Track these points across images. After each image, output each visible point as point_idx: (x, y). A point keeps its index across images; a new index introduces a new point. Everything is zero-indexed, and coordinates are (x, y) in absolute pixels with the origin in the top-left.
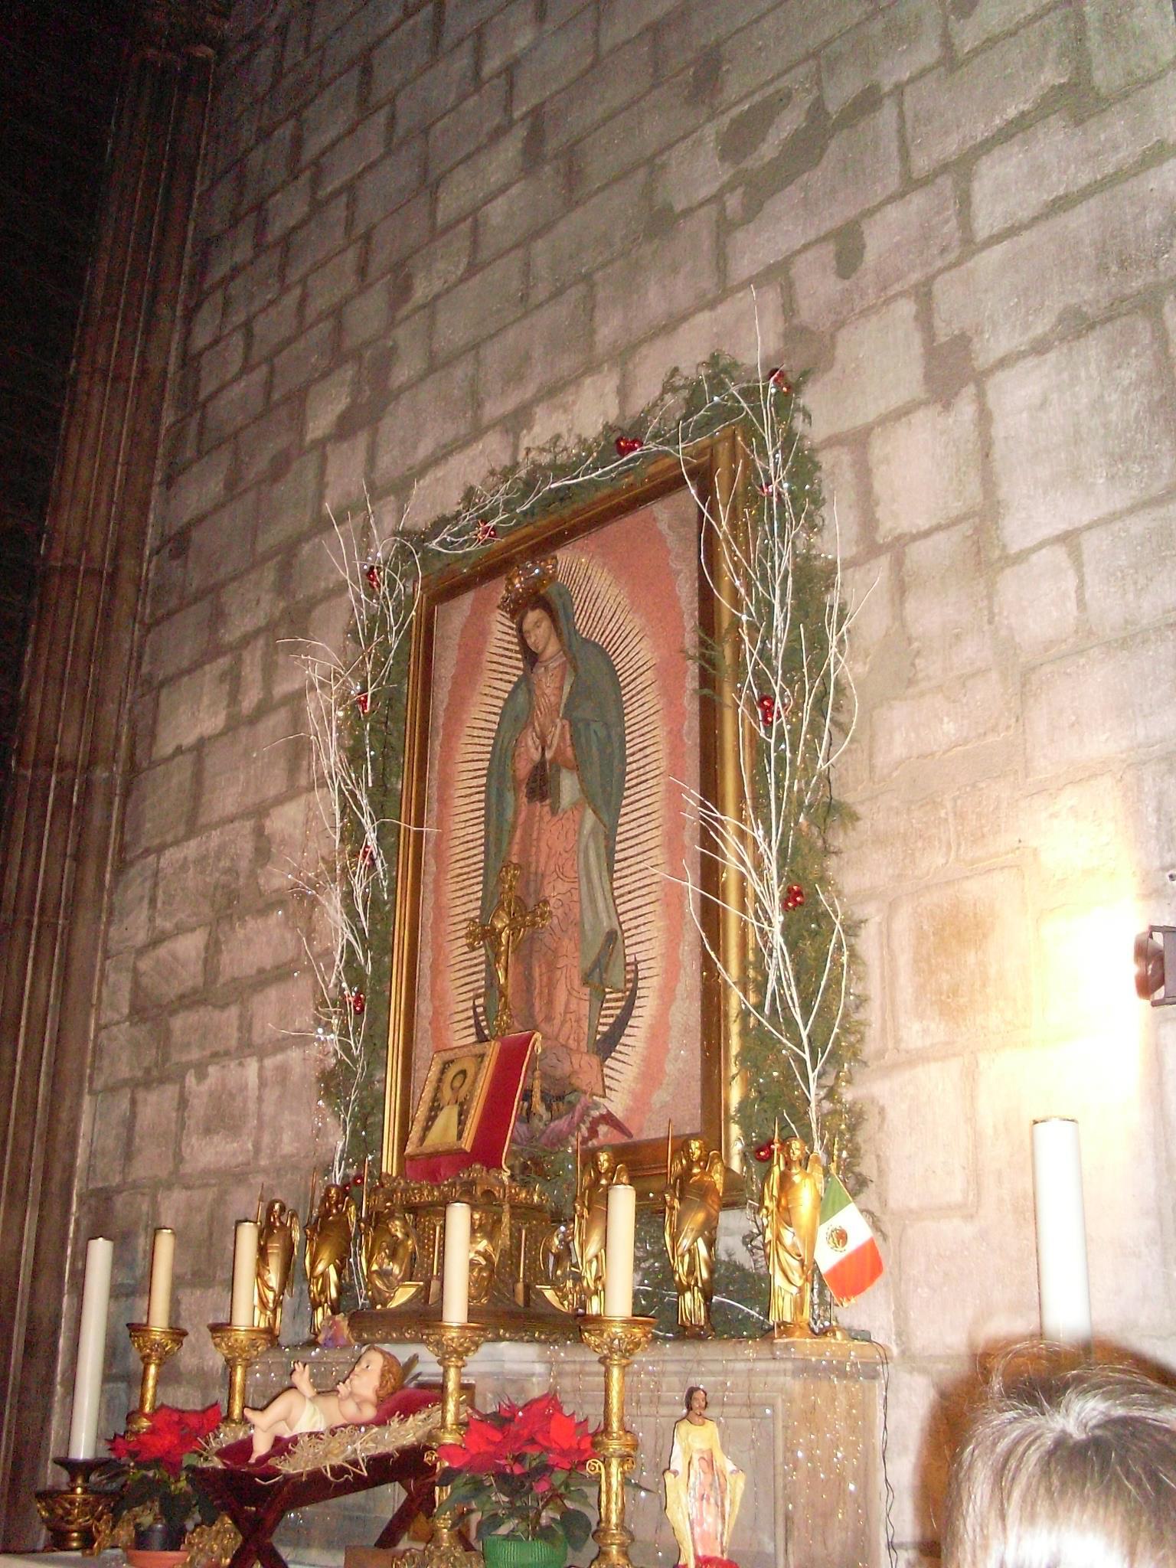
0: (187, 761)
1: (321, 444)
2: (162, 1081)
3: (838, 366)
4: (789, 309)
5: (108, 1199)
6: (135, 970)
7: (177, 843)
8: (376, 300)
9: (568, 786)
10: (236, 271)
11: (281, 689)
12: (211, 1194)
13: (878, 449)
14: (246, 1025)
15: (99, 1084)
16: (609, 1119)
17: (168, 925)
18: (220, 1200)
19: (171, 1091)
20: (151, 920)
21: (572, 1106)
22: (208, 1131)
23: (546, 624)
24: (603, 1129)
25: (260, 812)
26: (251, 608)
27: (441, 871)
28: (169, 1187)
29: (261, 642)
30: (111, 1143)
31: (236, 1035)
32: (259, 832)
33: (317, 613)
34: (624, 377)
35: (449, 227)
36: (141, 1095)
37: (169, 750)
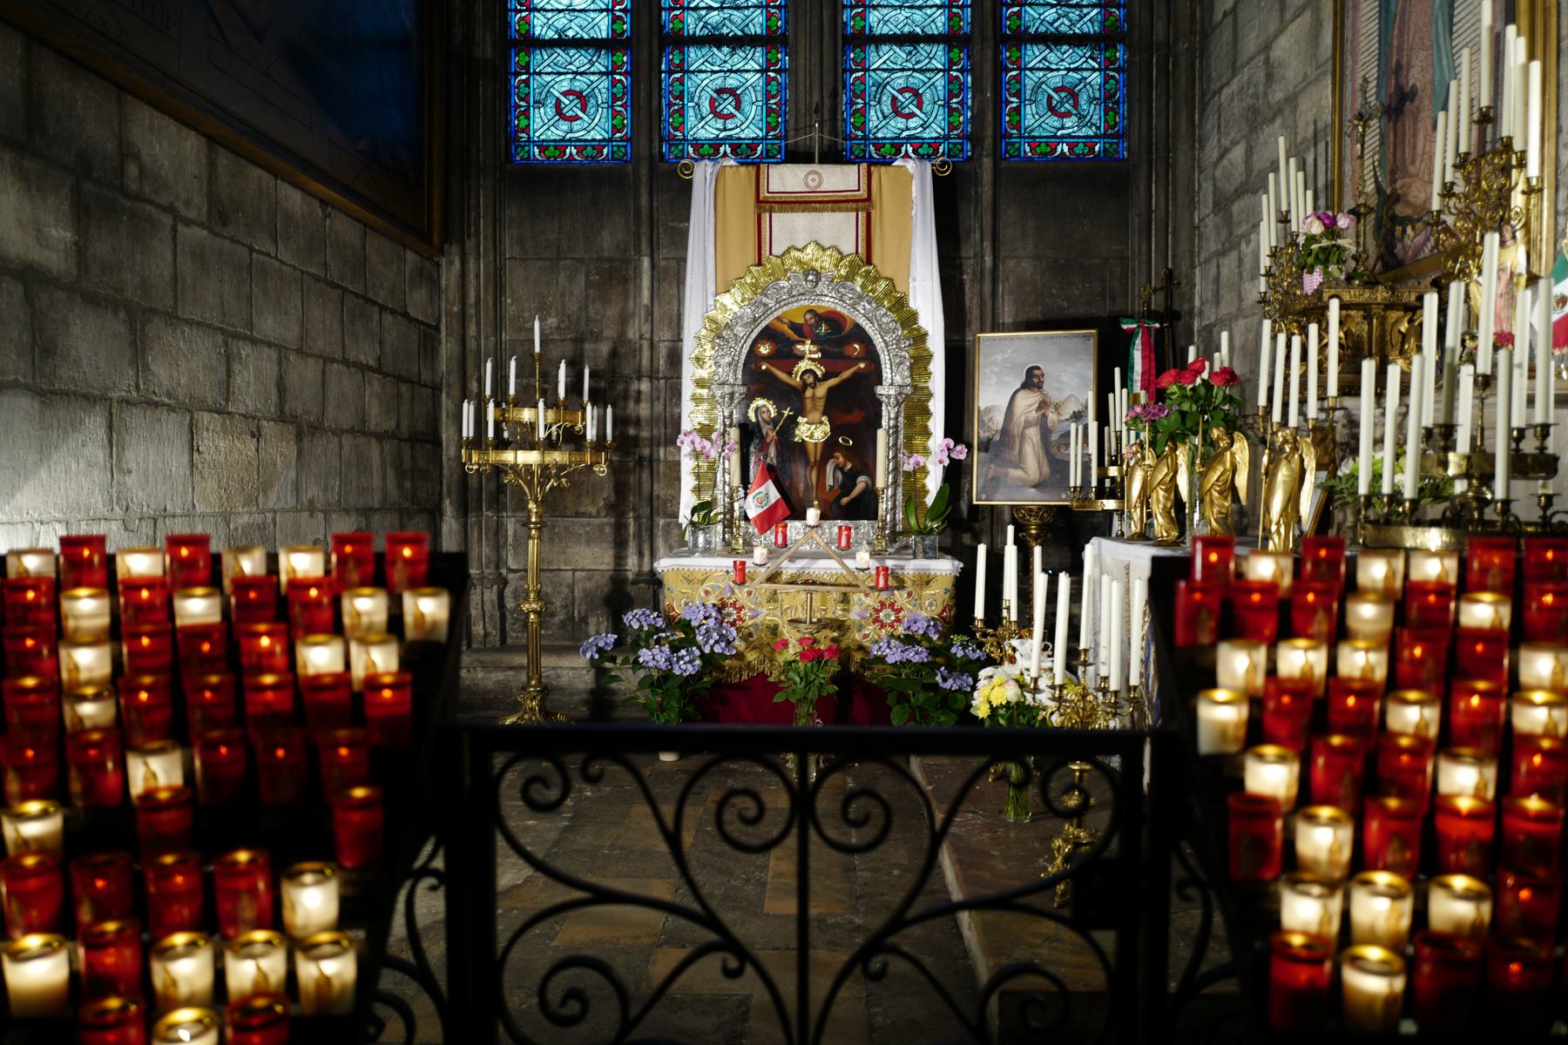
0: (1230, 19)
2: (1230, 250)
5: (1210, 332)
6: (1214, 178)
7: (1228, 83)
19: (1234, 254)
25: (1267, 47)
27: (1355, 62)
28: (1237, 318)
30: (1210, 295)
32: (1267, 61)
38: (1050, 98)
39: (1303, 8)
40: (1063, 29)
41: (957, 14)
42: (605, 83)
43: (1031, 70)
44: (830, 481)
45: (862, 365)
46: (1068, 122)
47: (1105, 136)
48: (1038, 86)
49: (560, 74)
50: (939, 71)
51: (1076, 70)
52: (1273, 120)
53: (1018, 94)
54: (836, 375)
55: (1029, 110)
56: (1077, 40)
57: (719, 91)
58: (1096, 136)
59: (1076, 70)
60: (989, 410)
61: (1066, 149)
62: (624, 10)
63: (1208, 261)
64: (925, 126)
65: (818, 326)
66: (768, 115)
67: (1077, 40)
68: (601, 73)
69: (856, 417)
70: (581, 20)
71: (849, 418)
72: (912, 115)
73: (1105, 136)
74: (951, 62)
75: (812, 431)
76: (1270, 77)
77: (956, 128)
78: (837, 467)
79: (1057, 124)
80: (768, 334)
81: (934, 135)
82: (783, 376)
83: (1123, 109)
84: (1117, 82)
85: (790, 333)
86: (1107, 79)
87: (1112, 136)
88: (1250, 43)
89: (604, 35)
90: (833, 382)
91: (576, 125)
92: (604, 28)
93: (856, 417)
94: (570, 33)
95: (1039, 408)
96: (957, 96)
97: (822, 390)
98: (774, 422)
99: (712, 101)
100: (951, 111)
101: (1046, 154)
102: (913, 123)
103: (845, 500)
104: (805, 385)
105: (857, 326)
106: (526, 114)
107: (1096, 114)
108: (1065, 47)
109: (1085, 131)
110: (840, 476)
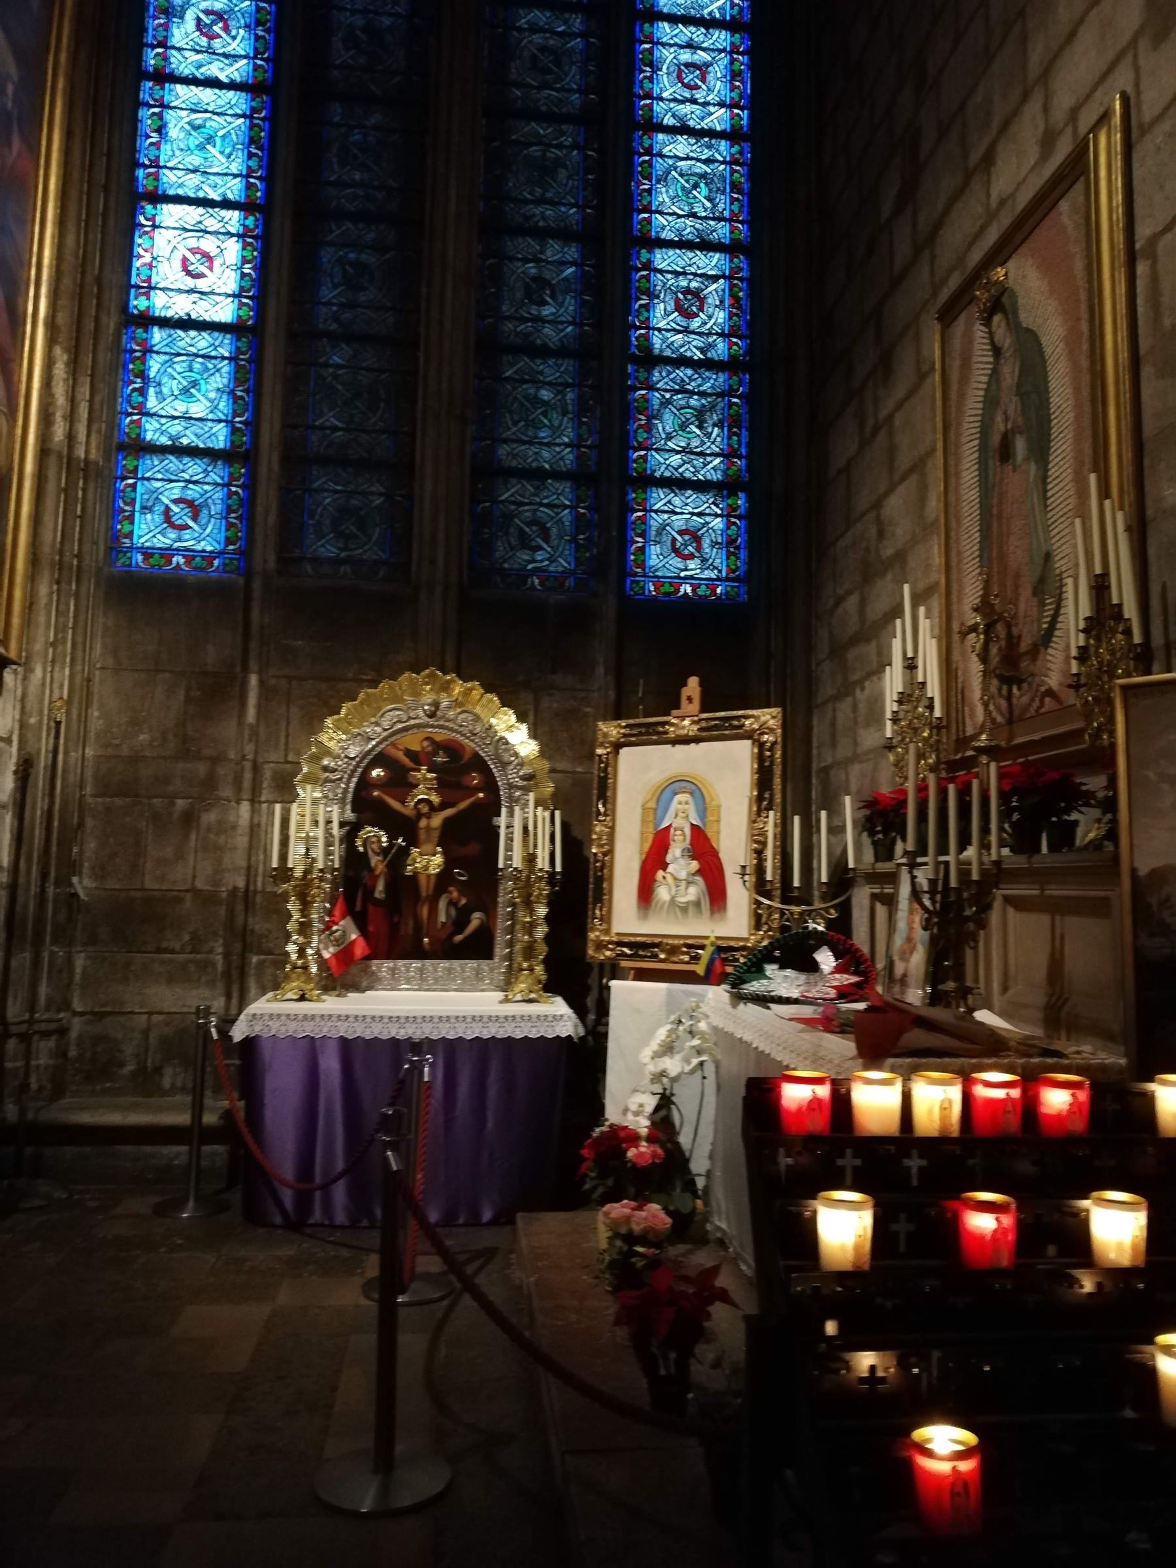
9: (1020, 445)
11: (883, 414)
15: (819, 701)
16: (1050, 693)
19: (849, 701)
21: (1030, 685)
23: (1003, 324)
24: (1047, 700)
25: (878, 505)
38: (674, 540)
39: (911, 470)
40: (688, 475)
42: (219, 494)
43: (656, 512)
44: (442, 918)
45: (481, 795)
46: (692, 564)
47: (727, 579)
48: (663, 527)
49: (172, 481)
50: (566, 507)
51: (700, 515)
54: (452, 805)
55: (654, 550)
56: (701, 487)
58: (718, 579)
59: (700, 515)
61: (689, 589)
63: (825, 703)
64: (552, 559)
65: (435, 754)
67: (701, 487)
68: (216, 484)
69: (473, 849)
70: (197, 428)
72: (540, 548)
73: (727, 579)
76: (881, 534)
78: (451, 903)
79: (680, 566)
80: (380, 759)
81: (560, 569)
82: (395, 804)
83: (743, 554)
84: (739, 528)
85: (406, 761)
86: (729, 524)
88: (863, 500)
89: (221, 445)
90: (449, 812)
91: (186, 534)
92: (222, 438)
93: (473, 849)
94: (185, 441)
97: (437, 821)
98: (385, 852)
100: (578, 547)
102: (539, 556)
104: (420, 815)
105: (476, 754)
106: (131, 519)
107: (718, 558)
108: (690, 492)
109: (707, 574)
110: (453, 912)
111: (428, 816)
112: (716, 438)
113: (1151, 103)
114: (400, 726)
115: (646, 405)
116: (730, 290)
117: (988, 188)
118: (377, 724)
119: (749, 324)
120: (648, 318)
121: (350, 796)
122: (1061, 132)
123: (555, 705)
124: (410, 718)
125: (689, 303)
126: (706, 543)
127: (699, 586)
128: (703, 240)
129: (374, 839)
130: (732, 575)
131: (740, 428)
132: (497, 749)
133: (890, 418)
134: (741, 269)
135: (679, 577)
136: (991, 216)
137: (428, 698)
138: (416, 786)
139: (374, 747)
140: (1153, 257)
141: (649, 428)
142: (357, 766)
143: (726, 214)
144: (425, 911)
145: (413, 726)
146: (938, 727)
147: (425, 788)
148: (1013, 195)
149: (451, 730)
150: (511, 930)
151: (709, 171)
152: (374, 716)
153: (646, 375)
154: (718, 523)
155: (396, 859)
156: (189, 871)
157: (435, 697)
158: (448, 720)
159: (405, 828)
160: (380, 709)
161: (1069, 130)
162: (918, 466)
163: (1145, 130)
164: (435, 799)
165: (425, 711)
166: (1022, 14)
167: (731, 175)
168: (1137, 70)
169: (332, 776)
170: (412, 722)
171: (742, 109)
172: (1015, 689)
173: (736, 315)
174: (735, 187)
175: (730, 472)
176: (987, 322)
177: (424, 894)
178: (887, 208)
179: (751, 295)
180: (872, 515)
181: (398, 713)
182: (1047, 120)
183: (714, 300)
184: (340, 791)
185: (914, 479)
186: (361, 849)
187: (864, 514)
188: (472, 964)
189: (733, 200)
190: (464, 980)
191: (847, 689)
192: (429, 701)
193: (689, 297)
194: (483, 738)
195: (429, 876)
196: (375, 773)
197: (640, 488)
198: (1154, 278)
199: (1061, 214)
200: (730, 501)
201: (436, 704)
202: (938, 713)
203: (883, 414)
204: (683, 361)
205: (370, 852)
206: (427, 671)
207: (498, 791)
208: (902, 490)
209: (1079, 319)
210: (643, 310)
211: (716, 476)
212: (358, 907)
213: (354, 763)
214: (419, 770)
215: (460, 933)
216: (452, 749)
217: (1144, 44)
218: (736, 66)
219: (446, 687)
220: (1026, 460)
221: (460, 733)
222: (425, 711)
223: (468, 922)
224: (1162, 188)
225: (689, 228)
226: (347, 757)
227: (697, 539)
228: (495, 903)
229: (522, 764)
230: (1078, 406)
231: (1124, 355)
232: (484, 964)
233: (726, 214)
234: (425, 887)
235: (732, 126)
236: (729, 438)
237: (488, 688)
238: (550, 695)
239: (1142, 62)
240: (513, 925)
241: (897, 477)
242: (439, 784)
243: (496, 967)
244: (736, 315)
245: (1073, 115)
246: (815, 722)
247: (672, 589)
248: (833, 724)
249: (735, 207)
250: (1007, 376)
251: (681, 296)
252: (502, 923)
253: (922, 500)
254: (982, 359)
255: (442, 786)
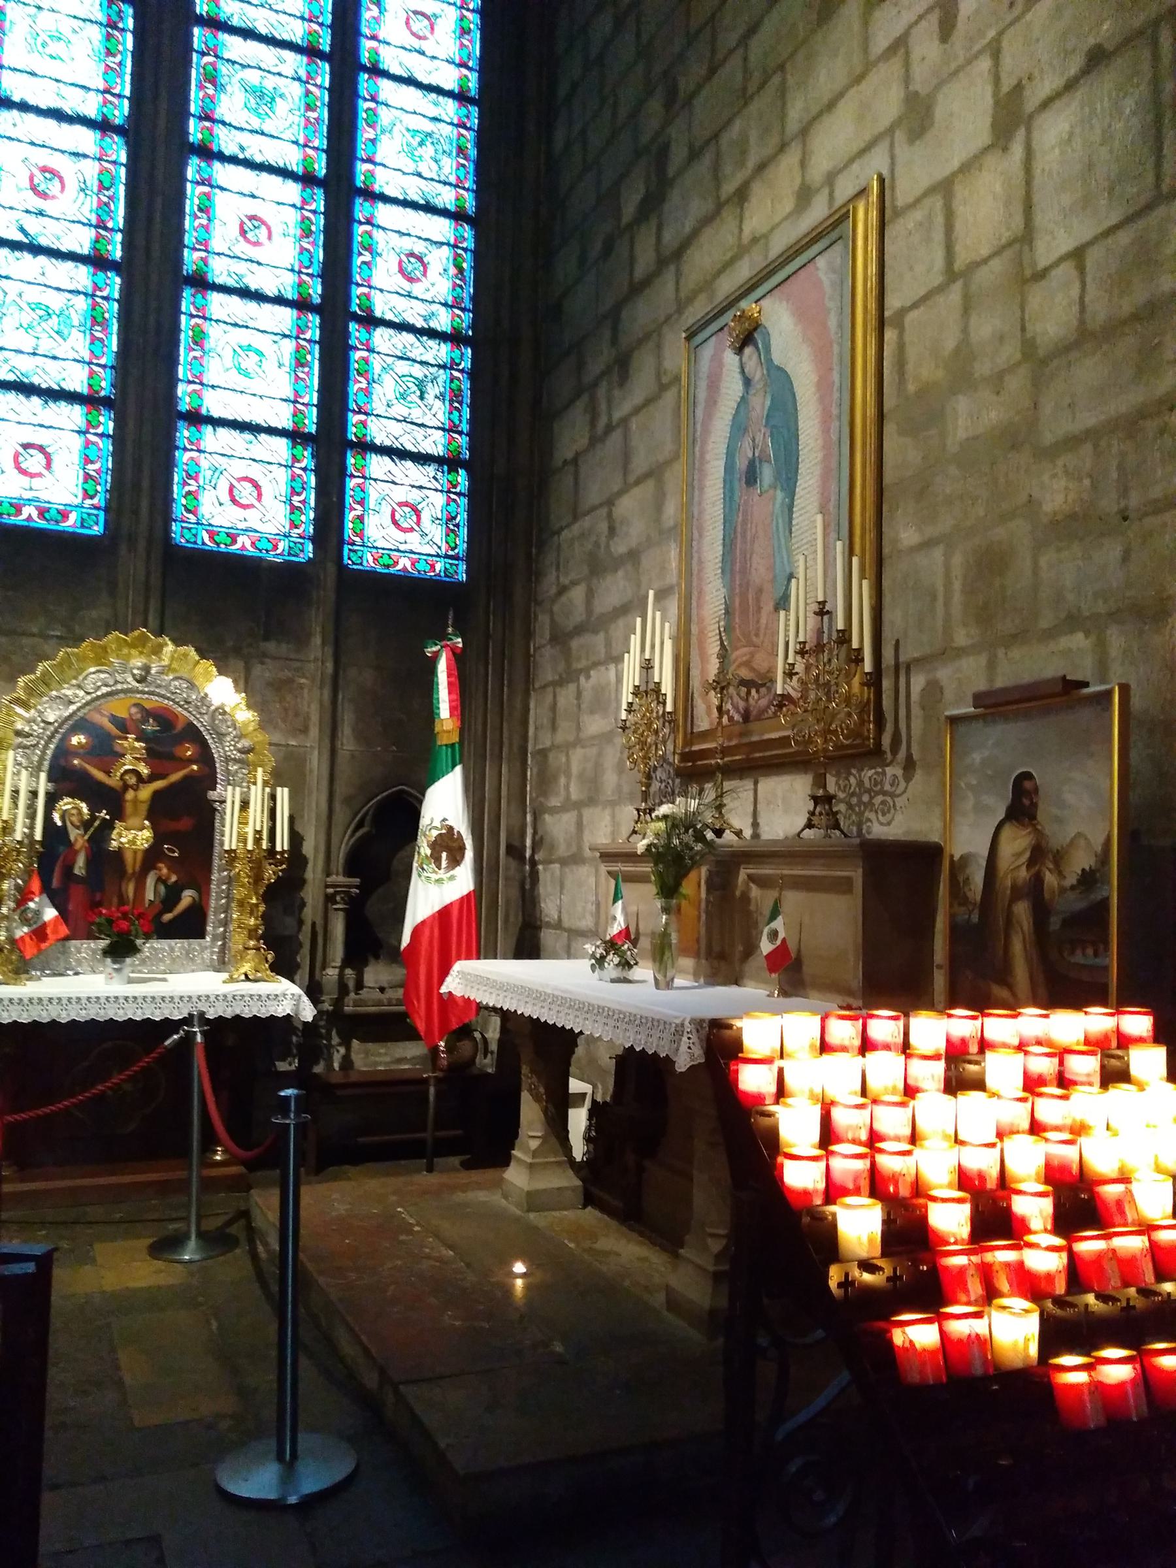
1: (630, 226)
3: (936, 125)
4: (907, 79)
7: (568, 526)
8: (655, 105)
9: (767, 474)
10: (574, 86)
11: (617, 415)
12: (594, 751)
13: (960, 191)
14: (608, 644)
15: (537, 685)
17: (567, 582)
18: (600, 754)
19: (572, 687)
20: (558, 577)
22: (592, 712)
23: (755, 357)
25: (610, 503)
26: (599, 359)
29: (604, 383)
31: (603, 651)
32: (610, 515)
33: (636, 354)
34: (804, 153)
35: (699, 31)
36: (558, 690)
37: (560, 464)
39: (648, 475)
41: (301, 412)
44: (150, 895)
45: (195, 767)
46: (409, 536)
47: (447, 556)
52: (616, 571)
53: (362, 503)
54: (163, 776)
57: (26, 446)
60: (965, 860)
62: (352, 509)
63: (544, 687)
65: (144, 721)
66: (86, 481)
69: (185, 824)
71: (173, 826)
74: (295, 459)
75: (132, 837)
76: (612, 531)
77: (296, 527)
78: (160, 880)
80: (79, 724)
82: (99, 775)
83: (464, 532)
85: (114, 731)
87: (451, 557)
88: (593, 494)
90: (159, 784)
93: (185, 824)
95: (1031, 863)
96: (299, 494)
97: (145, 793)
98: (86, 825)
99: (16, 456)
100: (293, 508)
101: (388, 567)
103: (168, 917)
104: (126, 787)
105: (191, 724)
107: (437, 533)
110: (162, 889)
111: (136, 788)
112: (439, 412)
113: (903, 193)
114: (104, 690)
115: (366, 367)
116: (455, 259)
117: (741, 222)
118: (79, 687)
119: (474, 299)
120: (370, 277)
121: (46, 764)
122: (818, 190)
123: (267, 674)
124: (116, 682)
125: (413, 266)
126: (426, 517)
127: (418, 561)
128: (428, 202)
129: (74, 812)
130: (451, 553)
131: (461, 403)
132: (213, 718)
133: (625, 421)
134: (465, 239)
135: (398, 550)
136: (741, 251)
137: (137, 662)
138: (123, 755)
139: (74, 713)
140: (901, 328)
141: (367, 392)
142: (56, 731)
143: (453, 179)
144: (130, 889)
145: (122, 691)
146: (669, 719)
147: (132, 758)
148: (766, 236)
149: (163, 696)
150: (226, 909)
151: (436, 131)
152: (75, 678)
153: (367, 336)
154: (439, 499)
155: (100, 835)
156: (718, 893)
157: (145, 661)
158: (159, 686)
159: (109, 801)
160: (83, 670)
161: (826, 191)
162: (655, 473)
163: (897, 214)
164: (145, 770)
165: (134, 675)
166: (781, 67)
167: (458, 139)
168: (893, 157)
169: (26, 742)
170: (119, 687)
171: (470, 69)
172: (753, 691)
173: (461, 287)
174: (461, 151)
175: (451, 448)
176: (739, 351)
177: (130, 870)
178: (629, 211)
179: (476, 268)
180: (604, 511)
181: (102, 676)
182: (803, 176)
183: (434, 269)
184: (36, 758)
185: (650, 484)
186: (59, 823)
187: (593, 509)
188: (178, 944)
189: (459, 165)
190: (173, 960)
191: (569, 676)
192: (139, 664)
193: (412, 260)
194: (197, 707)
195: (135, 852)
196: (75, 740)
197: (359, 453)
198: (901, 346)
199: (817, 269)
200: (450, 477)
201: (147, 669)
202: (669, 708)
203: (617, 415)
204: (403, 327)
205: (68, 824)
206: (136, 633)
207: (214, 762)
208: (636, 492)
209: (831, 369)
210: (364, 267)
211: (439, 451)
212: (55, 883)
213: (52, 728)
214: (126, 739)
215: (170, 912)
216: (164, 719)
217: (900, 136)
218: (465, 24)
219: (157, 650)
220: (773, 487)
221: (173, 700)
222: (134, 675)
223: (178, 899)
224: (911, 269)
225: (414, 190)
226: (43, 721)
227: (418, 513)
228: (209, 881)
229: (240, 737)
230: (826, 446)
231: (871, 411)
232: (195, 943)
233: (453, 179)
234: (131, 863)
235: (461, 87)
236: (451, 413)
237: (203, 654)
238: (262, 663)
239: (898, 151)
240: (228, 903)
241: (632, 479)
242: (148, 754)
243: (205, 948)
244: (461, 287)
245: (830, 179)
246: (532, 705)
247: (391, 562)
248: (554, 708)
249: (462, 172)
250: (758, 408)
251: (404, 258)
252: (214, 902)
253: (659, 507)
254: (732, 388)
255: (152, 755)
